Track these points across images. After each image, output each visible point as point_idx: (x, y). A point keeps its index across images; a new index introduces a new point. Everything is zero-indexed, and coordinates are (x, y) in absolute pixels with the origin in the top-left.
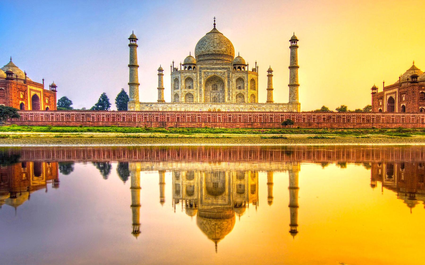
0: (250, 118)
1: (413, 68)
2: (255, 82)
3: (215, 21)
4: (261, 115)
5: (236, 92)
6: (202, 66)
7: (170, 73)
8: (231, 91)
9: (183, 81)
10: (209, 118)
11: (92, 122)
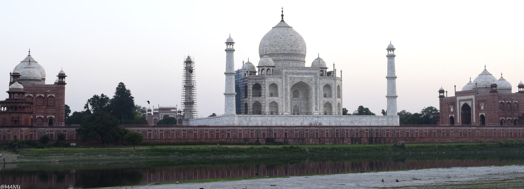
0: (357, 133)
1: (485, 73)
4: (367, 130)
5: (324, 101)
6: (288, 71)
8: (318, 99)
9: (267, 88)
10: (317, 133)
11: (194, 139)
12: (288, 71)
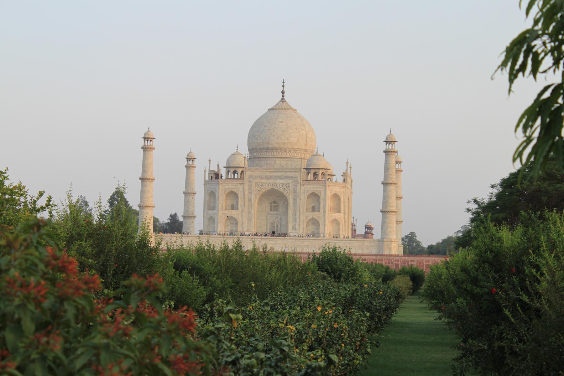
2: (340, 199)
3: (283, 86)
5: (307, 217)
6: (253, 174)
7: (203, 182)
8: (298, 214)
12: (253, 174)
